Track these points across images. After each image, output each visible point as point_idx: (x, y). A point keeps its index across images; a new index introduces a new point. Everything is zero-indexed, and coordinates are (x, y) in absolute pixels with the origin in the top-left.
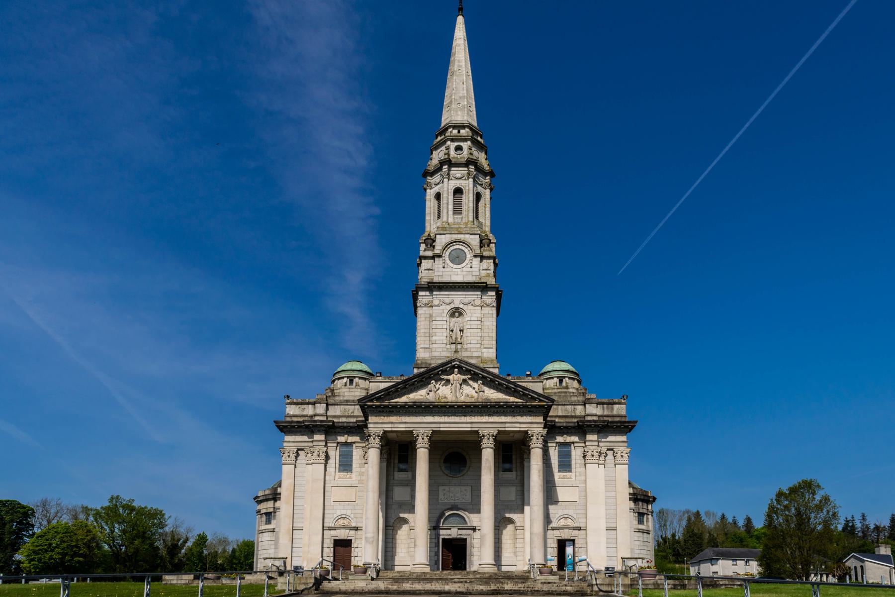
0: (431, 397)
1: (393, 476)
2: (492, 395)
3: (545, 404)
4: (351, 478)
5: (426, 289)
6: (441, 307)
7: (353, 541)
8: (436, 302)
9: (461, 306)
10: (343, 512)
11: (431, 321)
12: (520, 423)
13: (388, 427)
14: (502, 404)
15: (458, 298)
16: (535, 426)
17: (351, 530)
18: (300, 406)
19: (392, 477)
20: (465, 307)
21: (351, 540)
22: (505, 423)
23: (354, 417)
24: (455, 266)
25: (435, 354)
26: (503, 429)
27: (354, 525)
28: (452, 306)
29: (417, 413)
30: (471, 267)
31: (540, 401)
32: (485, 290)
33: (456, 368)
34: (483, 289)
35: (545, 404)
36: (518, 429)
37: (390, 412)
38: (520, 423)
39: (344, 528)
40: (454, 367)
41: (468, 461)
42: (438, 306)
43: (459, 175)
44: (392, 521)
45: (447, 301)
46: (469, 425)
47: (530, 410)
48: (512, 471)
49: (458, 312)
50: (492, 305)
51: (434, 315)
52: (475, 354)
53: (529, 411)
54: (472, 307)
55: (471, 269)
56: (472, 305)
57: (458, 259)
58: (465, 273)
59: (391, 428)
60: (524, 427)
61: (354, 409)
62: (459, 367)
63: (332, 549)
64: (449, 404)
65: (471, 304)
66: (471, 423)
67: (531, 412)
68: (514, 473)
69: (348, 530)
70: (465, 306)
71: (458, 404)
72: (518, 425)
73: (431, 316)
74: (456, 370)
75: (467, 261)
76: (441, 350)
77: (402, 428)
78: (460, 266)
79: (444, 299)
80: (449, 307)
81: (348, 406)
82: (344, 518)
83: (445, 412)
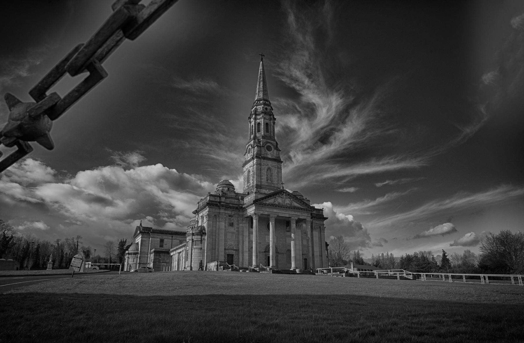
0: (277, 203)
2: (296, 204)
4: (233, 229)
6: (264, 166)
7: (234, 255)
8: (262, 164)
9: (271, 167)
10: (231, 243)
11: (261, 170)
12: (304, 216)
13: (262, 212)
15: (270, 163)
16: (308, 217)
17: (234, 250)
18: (214, 197)
20: (272, 168)
21: (234, 255)
23: (234, 204)
24: (268, 152)
25: (263, 184)
27: (235, 248)
28: (268, 166)
29: (272, 208)
30: (274, 153)
31: (311, 209)
36: (303, 218)
38: (304, 216)
39: (232, 249)
40: (284, 193)
42: (263, 165)
43: (267, 118)
46: (288, 215)
49: (269, 169)
51: (262, 169)
52: (276, 186)
54: (274, 168)
55: (274, 154)
57: (269, 148)
58: (272, 155)
60: (305, 218)
61: (234, 201)
63: (227, 258)
66: (289, 214)
69: (233, 251)
72: (303, 216)
73: (261, 169)
74: (284, 194)
76: (265, 182)
77: (266, 213)
78: (270, 152)
81: (232, 200)
82: (231, 246)
83: (280, 209)
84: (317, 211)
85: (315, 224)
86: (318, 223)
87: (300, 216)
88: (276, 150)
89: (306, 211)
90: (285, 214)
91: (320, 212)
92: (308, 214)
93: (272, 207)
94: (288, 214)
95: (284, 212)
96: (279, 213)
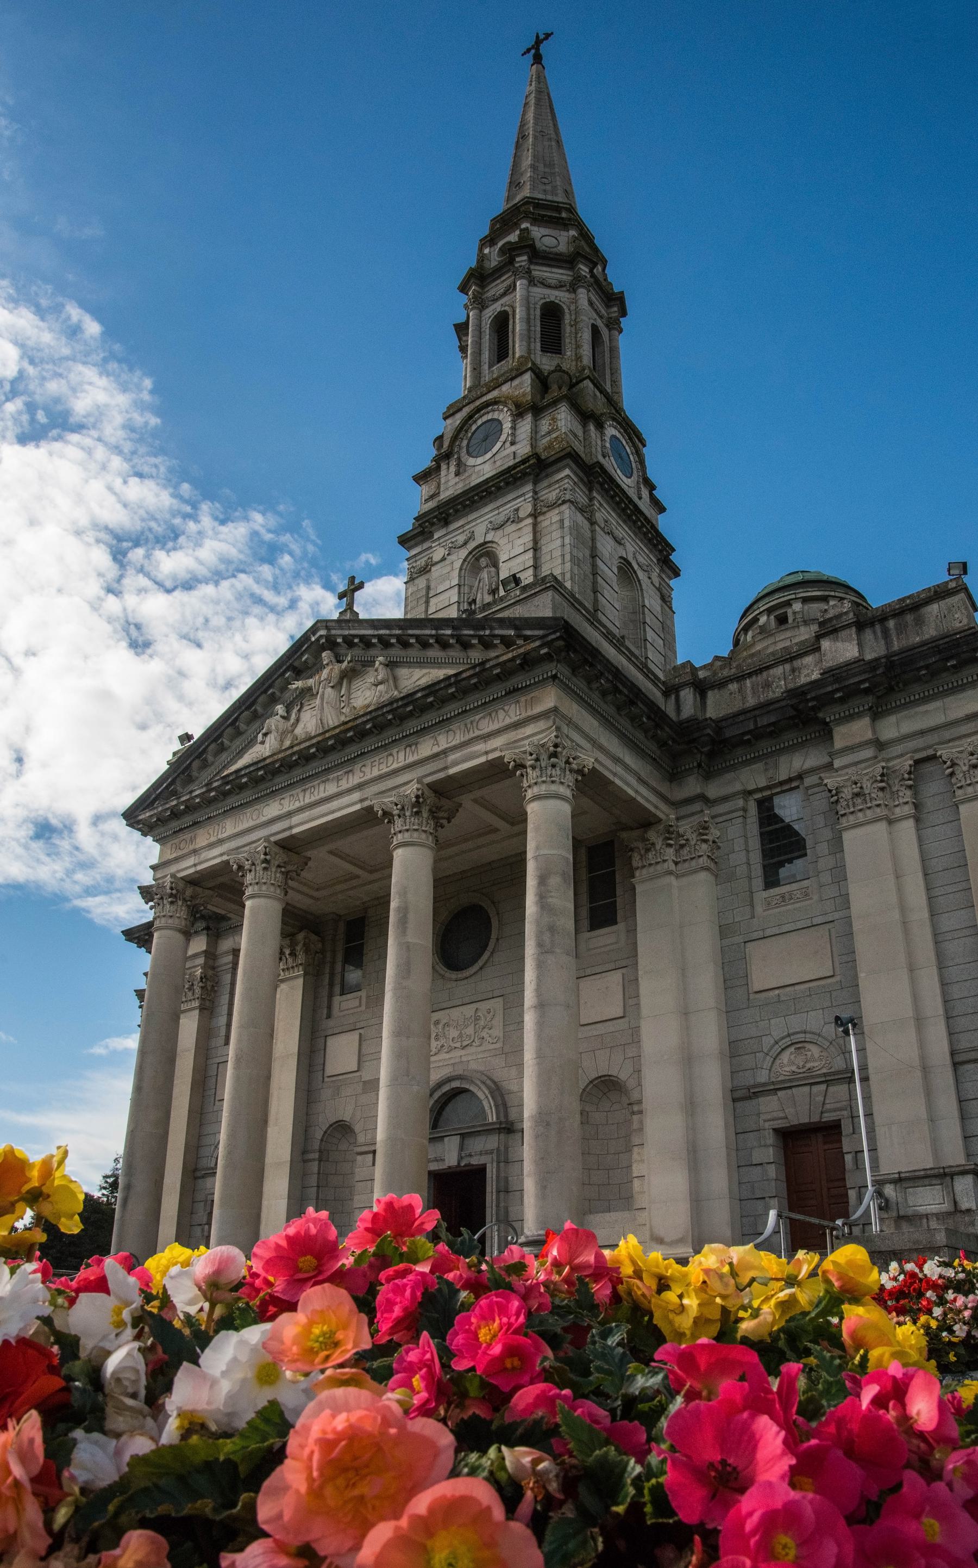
1: (329, 1007)
3: (537, 643)
5: (420, 538)
14: (419, 695)
19: (325, 1011)
22: (445, 752)
24: (480, 460)
26: (441, 775)
32: (544, 474)
33: (323, 648)
34: (537, 475)
35: (537, 643)
36: (483, 759)
37: (195, 823)
41: (495, 923)
44: (319, 1135)
45: (461, 539)
46: (356, 796)
47: (509, 684)
48: (616, 923)
50: (560, 502)
53: (509, 693)
56: (513, 522)
59: (195, 865)
62: (331, 644)
64: (296, 749)
65: (509, 523)
66: (360, 787)
67: (516, 690)
68: (621, 926)
70: (500, 532)
71: (314, 741)
72: (480, 747)
75: (503, 438)
79: (453, 540)
80: (463, 553)
84: (891, 624)
85: (868, 753)
86: (908, 727)
87: (452, 757)
88: (529, 418)
89: (498, 690)
90: (335, 804)
91: (920, 622)
92: (533, 702)
93: (247, 795)
94: (350, 791)
95: (331, 789)
96: (290, 814)
